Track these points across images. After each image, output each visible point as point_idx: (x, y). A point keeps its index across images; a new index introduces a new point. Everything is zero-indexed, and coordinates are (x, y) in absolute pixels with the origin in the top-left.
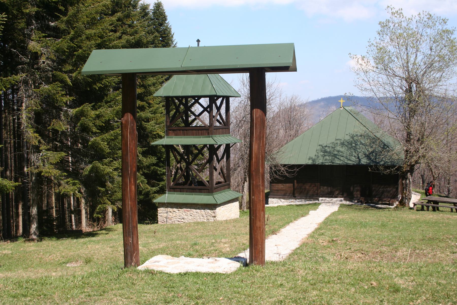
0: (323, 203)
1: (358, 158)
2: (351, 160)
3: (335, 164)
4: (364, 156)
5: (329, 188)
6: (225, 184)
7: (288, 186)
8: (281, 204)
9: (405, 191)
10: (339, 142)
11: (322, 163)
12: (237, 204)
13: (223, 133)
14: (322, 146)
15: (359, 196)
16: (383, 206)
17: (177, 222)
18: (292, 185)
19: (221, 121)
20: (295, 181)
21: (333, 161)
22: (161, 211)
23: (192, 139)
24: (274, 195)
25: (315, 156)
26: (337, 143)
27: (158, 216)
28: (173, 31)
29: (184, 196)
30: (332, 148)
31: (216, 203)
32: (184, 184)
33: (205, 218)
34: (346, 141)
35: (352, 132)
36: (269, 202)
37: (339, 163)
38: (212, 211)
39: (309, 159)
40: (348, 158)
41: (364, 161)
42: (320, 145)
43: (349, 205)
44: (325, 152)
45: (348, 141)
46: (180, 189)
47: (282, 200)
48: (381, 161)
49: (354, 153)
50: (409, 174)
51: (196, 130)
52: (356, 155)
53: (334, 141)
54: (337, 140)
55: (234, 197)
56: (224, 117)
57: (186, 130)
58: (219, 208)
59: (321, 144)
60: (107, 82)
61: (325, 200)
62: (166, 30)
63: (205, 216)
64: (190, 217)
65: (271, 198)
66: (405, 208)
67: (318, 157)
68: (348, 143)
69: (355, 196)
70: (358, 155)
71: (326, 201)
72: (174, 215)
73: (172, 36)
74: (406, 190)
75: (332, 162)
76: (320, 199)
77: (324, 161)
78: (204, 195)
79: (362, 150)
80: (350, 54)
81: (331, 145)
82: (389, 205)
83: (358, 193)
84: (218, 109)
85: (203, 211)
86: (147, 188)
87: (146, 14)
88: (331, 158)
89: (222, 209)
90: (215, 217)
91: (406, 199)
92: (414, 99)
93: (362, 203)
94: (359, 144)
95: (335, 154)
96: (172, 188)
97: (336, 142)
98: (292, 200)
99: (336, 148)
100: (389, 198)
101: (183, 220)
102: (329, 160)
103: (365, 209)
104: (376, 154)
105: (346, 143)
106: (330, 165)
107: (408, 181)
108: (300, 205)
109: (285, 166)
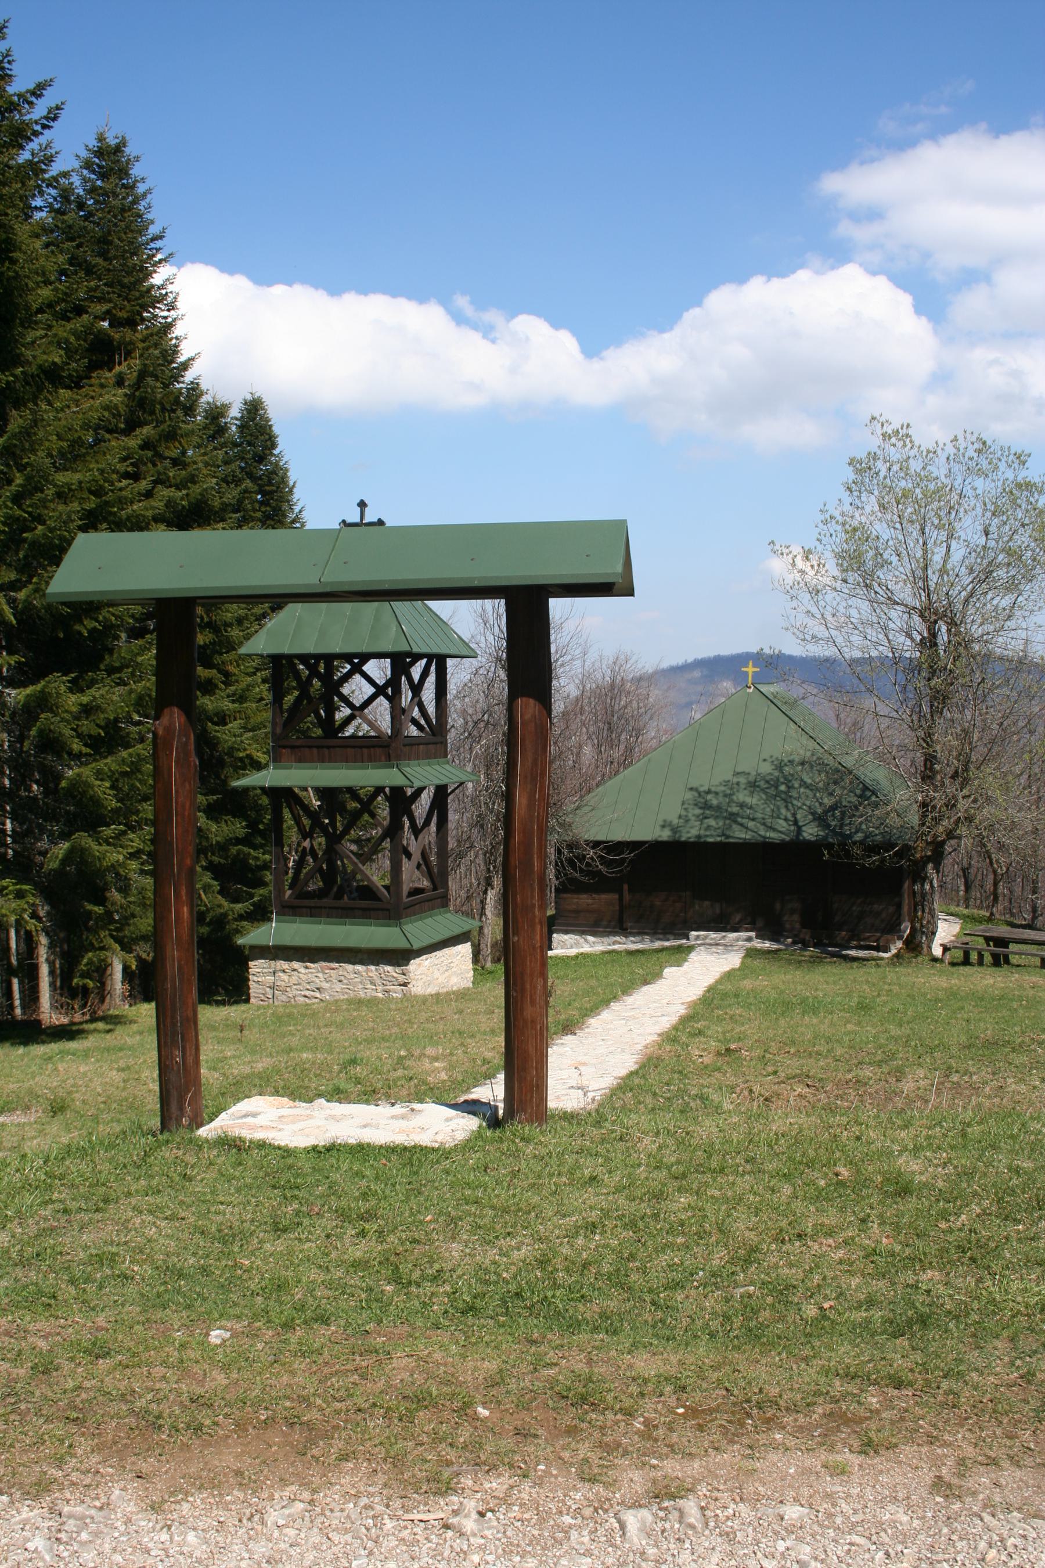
0: (700, 945)
1: (796, 822)
2: (774, 830)
3: (731, 840)
4: (810, 817)
6: (435, 896)
7: (605, 900)
8: (586, 949)
9: (920, 913)
10: (742, 780)
11: (699, 837)
12: (465, 950)
13: (428, 756)
14: (696, 790)
15: (797, 926)
16: (861, 953)
17: (302, 999)
18: (617, 896)
19: (423, 722)
20: (626, 887)
21: (728, 833)
22: (259, 970)
23: (344, 772)
25: (680, 817)
26: (738, 784)
27: (251, 983)
28: (293, 476)
29: (320, 927)
30: (725, 796)
31: (408, 946)
32: (321, 894)
33: (380, 988)
34: (763, 778)
35: (777, 754)
36: (554, 944)
37: (743, 836)
38: (398, 970)
39: (663, 827)
40: (767, 823)
41: (810, 831)
42: (691, 789)
43: (769, 952)
44: (706, 806)
45: (768, 778)
46: (311, 908)
47: (591, 938)
48: (857, 832)
49: (783, 811)
50: (930, 866)
51: (354, 747)
52: (789, 816)
53: (728, 776)
54: (737, 774)
55: (457, 931)
56: (431, 710)
57: (328, 747)
58: (418, 961)
59: (694, 785)
60: (113, 615)
61: (706, 937)
62: (274, 472)
63: (378, 981)
64: (338, 987)
65: (558, 932)
66: (920, 959)
67: (687, 821)
68: (767, 782)
69: (788, 926)
70: (794, 815)
71: (708, 941)
72: (294, 979)
73: (291, 491)
74: (923, 911)
75: (723, 835)
76: (693, 934)
77: (702, 832)
78: (376, 925)
79: (805, 802)
80: (773, 542)
81: (723, 788)
82: (878, 949)
83: (796, 917)
84: (417, 689)
85: (373, 968)
86: (220, 906)
87: (222, 430)
88: (721, 823)
89: (427, 963)
90: (405, 985)
91: (923, 933)
92: (942, 665)
93: (805, 945)
94: (796, 785)
95: (732, 814)
96: (288, 907)
97: (735, 780)
98: (617, 938)
99: (735, 798)
100: (876, 931)
101: (317, 995)
102: (716, 829)
103: (815, 961)
104: (843, 813)
105: (762, 784)
106: (720, 843)
107: (927, 887)
108: (638, 951)
109: (596, 844)
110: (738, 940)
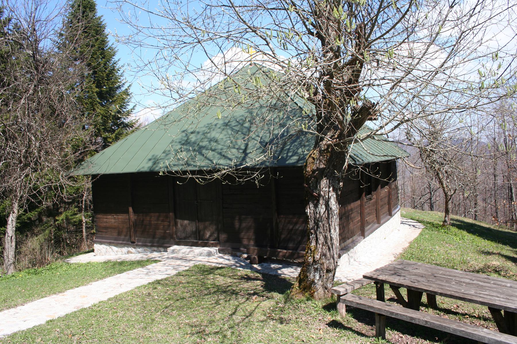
5: (194, 224)
9: (313, 244)
20: (131, 209)
24: (102, 238)
83: (251, 234)
95: (201, 148)
107: (322, 209)
110: (201, 254)
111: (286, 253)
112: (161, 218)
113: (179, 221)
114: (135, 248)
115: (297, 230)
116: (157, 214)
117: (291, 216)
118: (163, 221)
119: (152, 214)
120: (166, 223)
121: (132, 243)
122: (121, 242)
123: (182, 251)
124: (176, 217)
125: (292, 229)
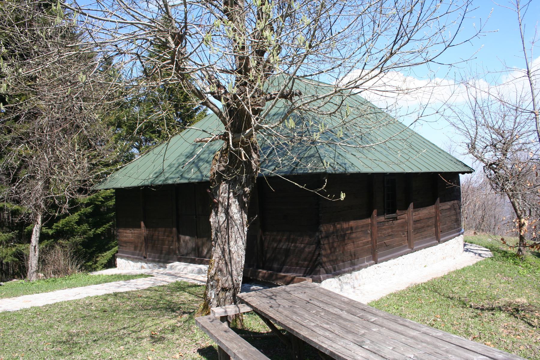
20: (142, 224)
65: (122, 257)
110: (192, 272)
111: (265, 273)
112: (167, 234)
113: (182, 237)
114: (146, 263)
115: (281, 248)
116: (163, 229)
117: (275, 233)
118: (168, 236)
119: (160, 229)
120: (170, 239)
121: (144, 259)
122: (136, 257)
123: (179, 267)
124: (179, 232)
125: (276, 248)
